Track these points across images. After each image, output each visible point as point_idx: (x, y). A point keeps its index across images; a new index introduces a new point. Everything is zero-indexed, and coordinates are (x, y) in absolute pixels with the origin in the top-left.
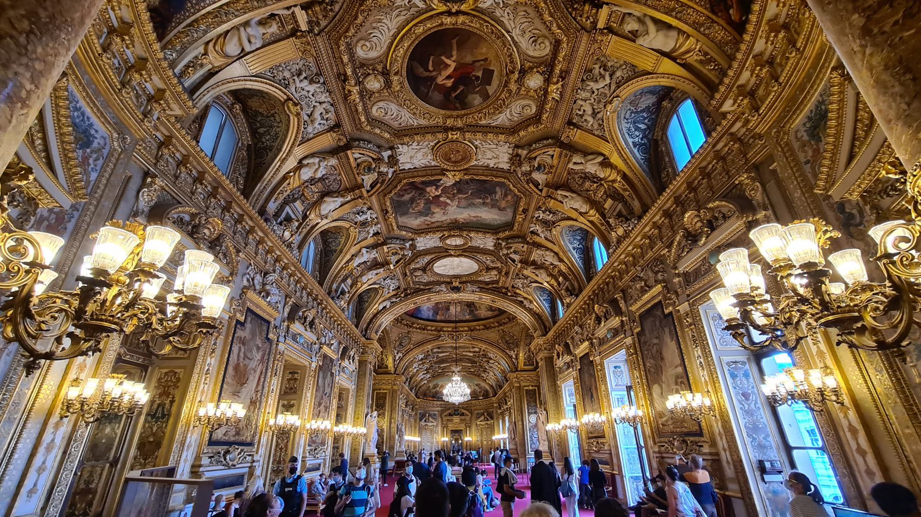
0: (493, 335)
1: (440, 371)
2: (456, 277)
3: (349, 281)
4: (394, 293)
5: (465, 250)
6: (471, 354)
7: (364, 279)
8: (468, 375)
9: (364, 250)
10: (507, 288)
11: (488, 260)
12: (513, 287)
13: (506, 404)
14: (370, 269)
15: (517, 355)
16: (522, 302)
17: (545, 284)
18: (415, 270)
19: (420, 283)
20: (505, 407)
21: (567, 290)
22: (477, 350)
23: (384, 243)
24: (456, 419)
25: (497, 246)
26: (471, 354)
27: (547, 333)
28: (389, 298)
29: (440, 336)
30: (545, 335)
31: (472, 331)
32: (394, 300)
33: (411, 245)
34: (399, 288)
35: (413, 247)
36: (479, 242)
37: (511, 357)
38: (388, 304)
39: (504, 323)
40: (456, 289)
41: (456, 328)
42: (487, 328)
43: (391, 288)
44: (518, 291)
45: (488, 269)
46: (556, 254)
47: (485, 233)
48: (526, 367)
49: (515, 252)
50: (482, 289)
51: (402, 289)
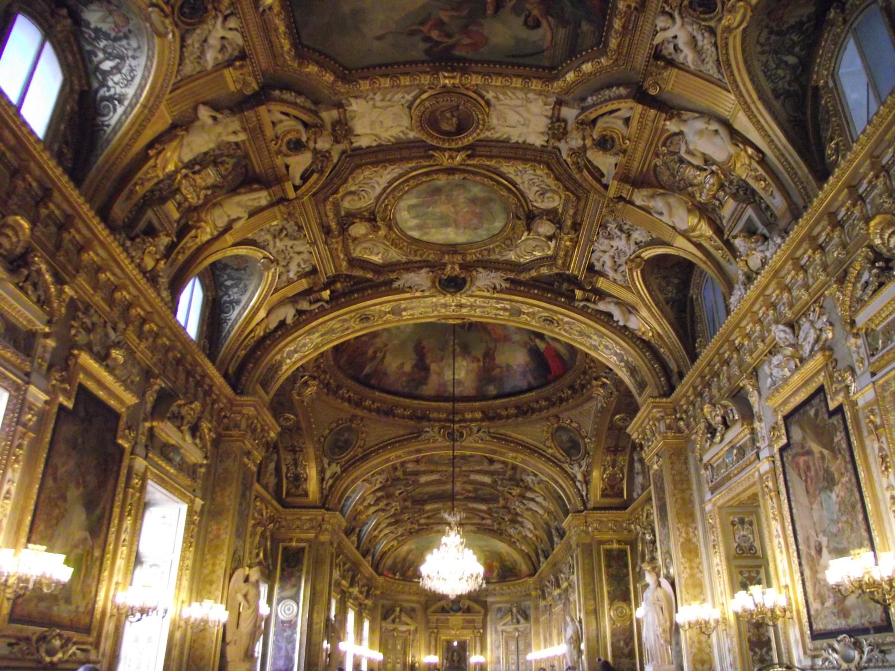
0: (534, 432)
1: (420, 516)
2: (452, 249)
3: (172, 209)
4: (304, 284)
5: (472, 150)
6: (487, 479)
7: (218, 218)
8: (479, 529)
9: (204, 113)
10: (573, 281)
11: (530, 180)
12: (591, 268)
13: (558, 586)
14: (234, 191)
15: (587, 476)
16: (610, 315)
17: (681, 242)
18: (351, 217)
19: (365, 264)
20: (557, 592)
21: (750, 232)
22: (497, 466)
23: (261, 97)
24: (456, 619)
25: (557, 128)
26: (487, 479)
27: (672, 389)
28: (293, 300)
29: (420, 432)
30: (667, 395)
31: (491, 419)
32: (304, 305)
33: (335, 124)
34: (314, 271)
35: (342, 130)
36: (513, 118)
37: (573, 479)
38: (288, 313)
39: (561, 400)
40: (454, 285)
41: (454, 412)
42: (523, 411)
43: (293, 267)
44: (601, 283)
45: (530, 218)
46: (726, 124)
47: (526, 78)
48: (607, 501)
49: (605, 144)
50: (516, 286)
51: (323, 279)
